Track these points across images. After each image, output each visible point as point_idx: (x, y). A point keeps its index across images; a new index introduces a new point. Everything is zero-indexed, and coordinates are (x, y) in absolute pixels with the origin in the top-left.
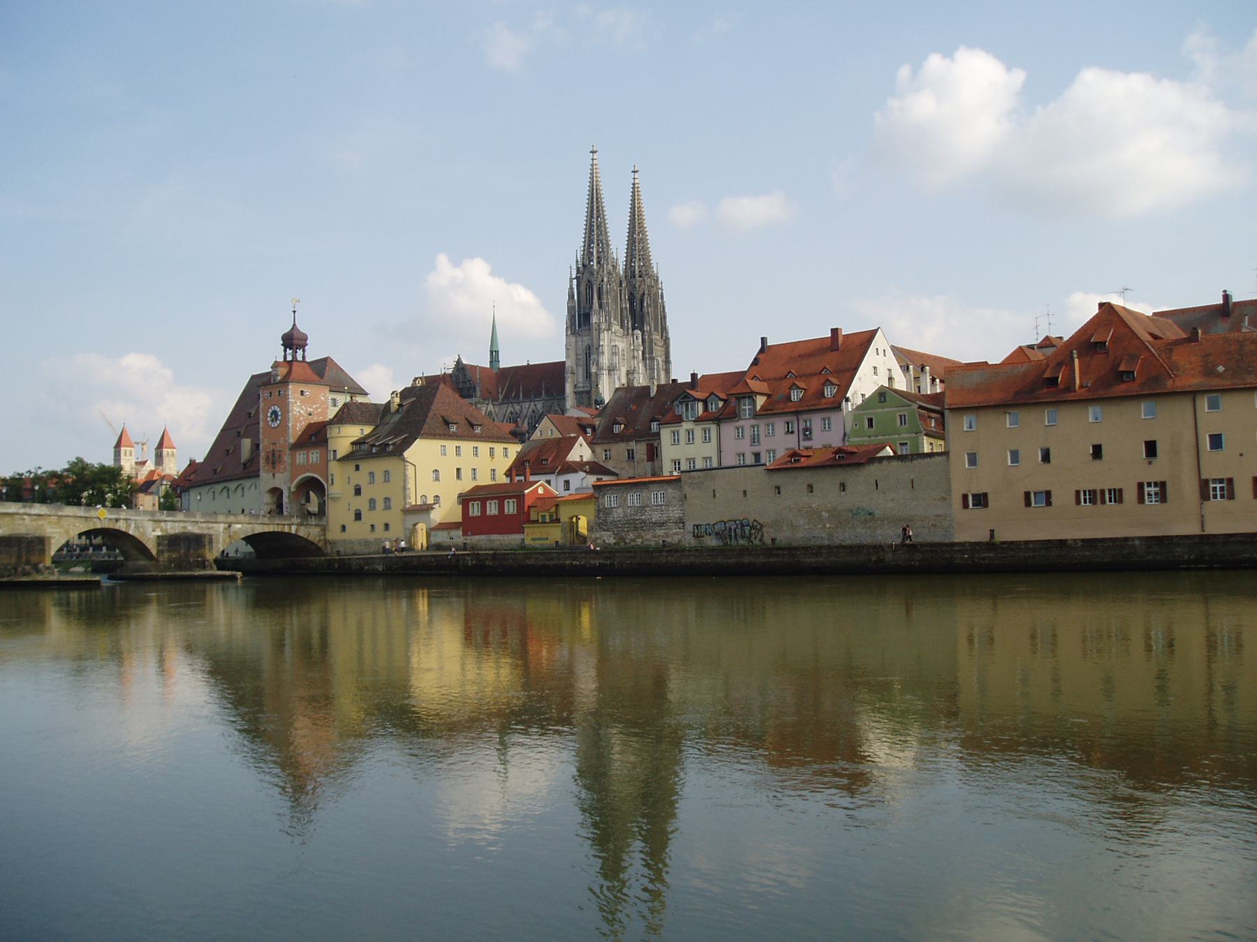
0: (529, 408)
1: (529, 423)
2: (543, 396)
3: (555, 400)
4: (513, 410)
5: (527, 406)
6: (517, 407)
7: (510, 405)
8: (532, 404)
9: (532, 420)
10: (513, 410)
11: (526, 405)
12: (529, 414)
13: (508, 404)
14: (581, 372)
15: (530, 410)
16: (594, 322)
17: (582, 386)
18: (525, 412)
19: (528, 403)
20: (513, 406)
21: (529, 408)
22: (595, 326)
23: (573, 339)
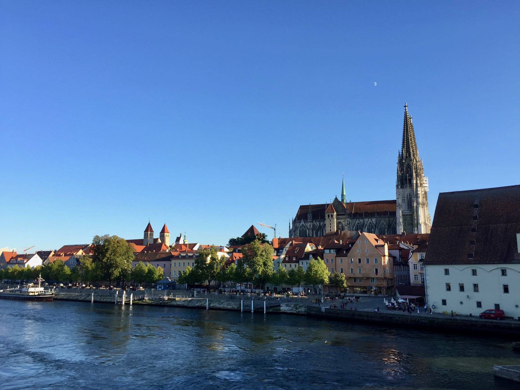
0: (368, 221)
1: (368, 228)
2: (376, 216)
3: (383, 218)
4: (359, 222)
5: (367, 220)
6: (361, 221)
7: (358, 219)
8: (370, 219)
9: (369, 227)
10: (359, 222)
11: (366, 220)
12: (368, 224)
13: (357, 219)
14: (405, 206)
15: (369, 222)
16: (414, 183)
17: (407, 212)
18: (366, 223)
19: (368, 219)
20: (359, 220)
21: (368, 221)
22: (415, 185)
23: (401, 190)
